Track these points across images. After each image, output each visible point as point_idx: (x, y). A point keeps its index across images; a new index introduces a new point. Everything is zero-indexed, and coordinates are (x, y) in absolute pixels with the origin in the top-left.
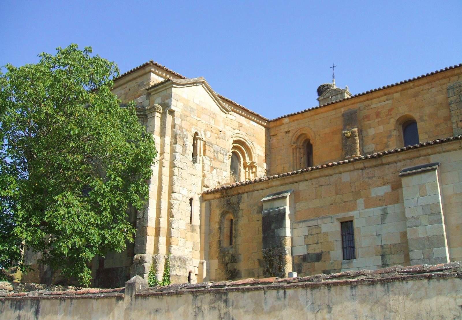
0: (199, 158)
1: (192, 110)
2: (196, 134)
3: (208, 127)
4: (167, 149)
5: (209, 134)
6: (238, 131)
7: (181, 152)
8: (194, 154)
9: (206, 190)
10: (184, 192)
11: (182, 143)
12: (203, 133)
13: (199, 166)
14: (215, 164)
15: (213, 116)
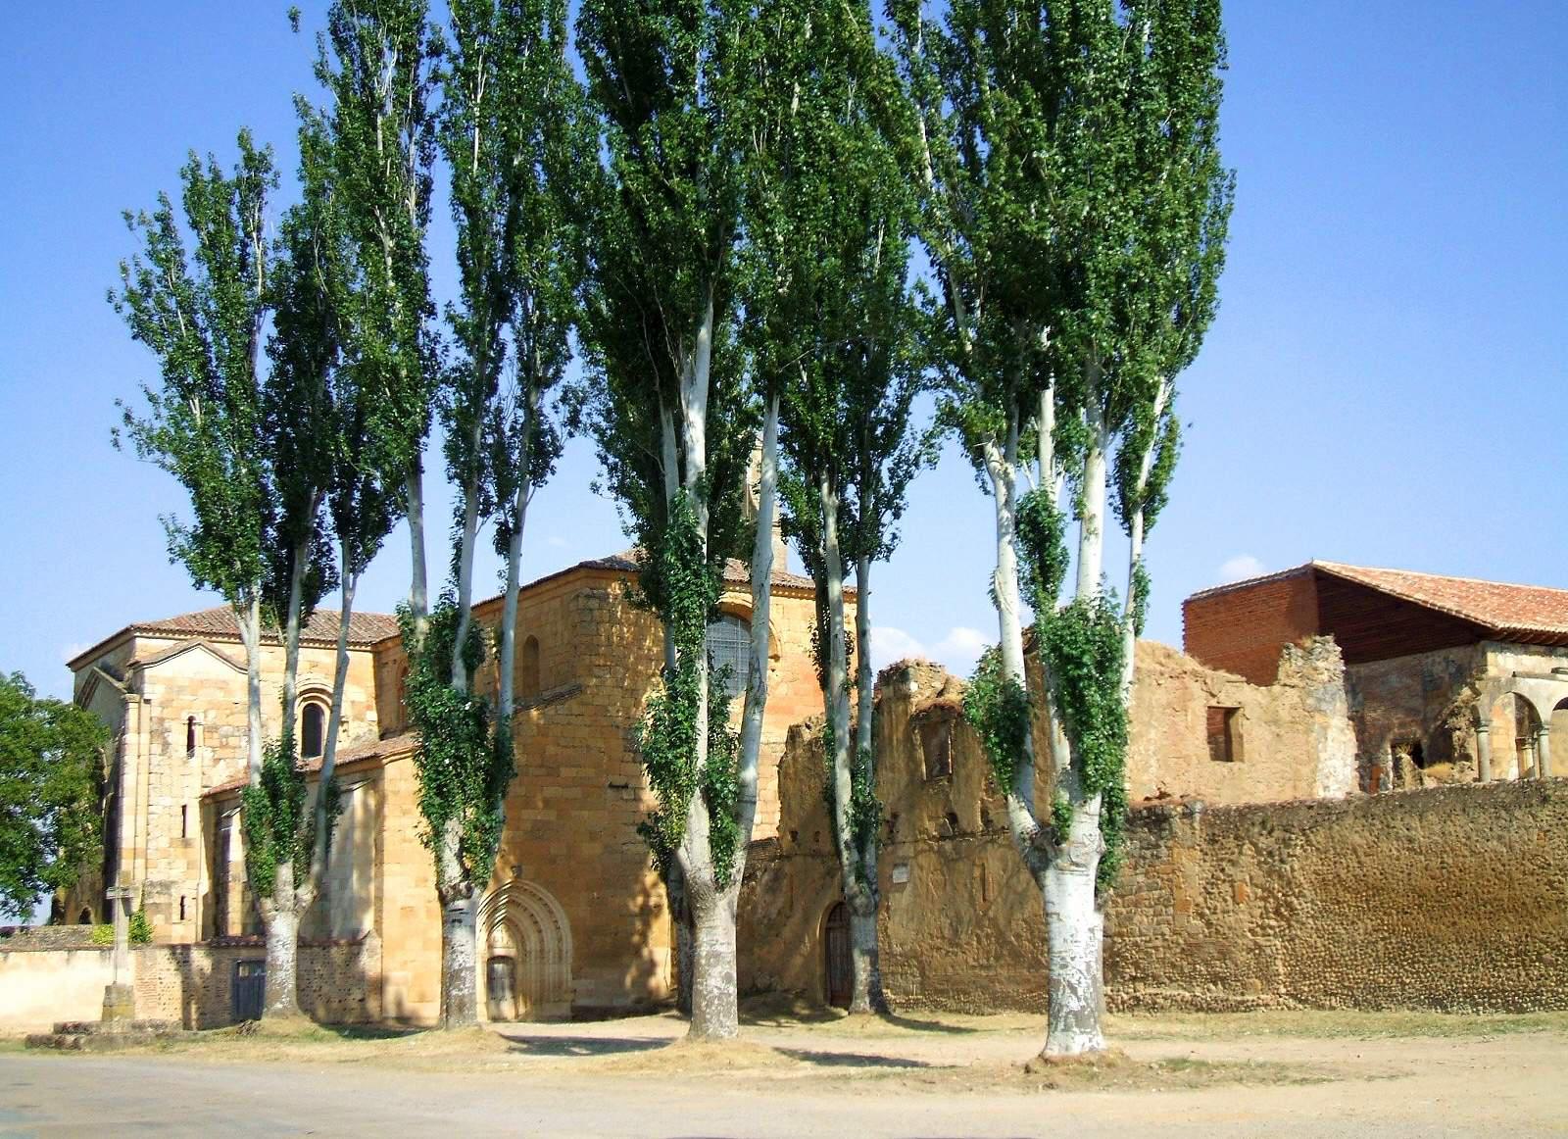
0: (197, 749)
1: (181, 690)
2: (191, 719)
3: (216, 706)
4: (144, 751)
5: (212, 714)
6: (309, 676)
7: (159, 751)
8: (190, 746)
9: (206, 790)
10: (168, 801)
11: (160, 741)
12: (202, 716)
13: (195, 761)
14: (220, 753)
15: (223, 686)
